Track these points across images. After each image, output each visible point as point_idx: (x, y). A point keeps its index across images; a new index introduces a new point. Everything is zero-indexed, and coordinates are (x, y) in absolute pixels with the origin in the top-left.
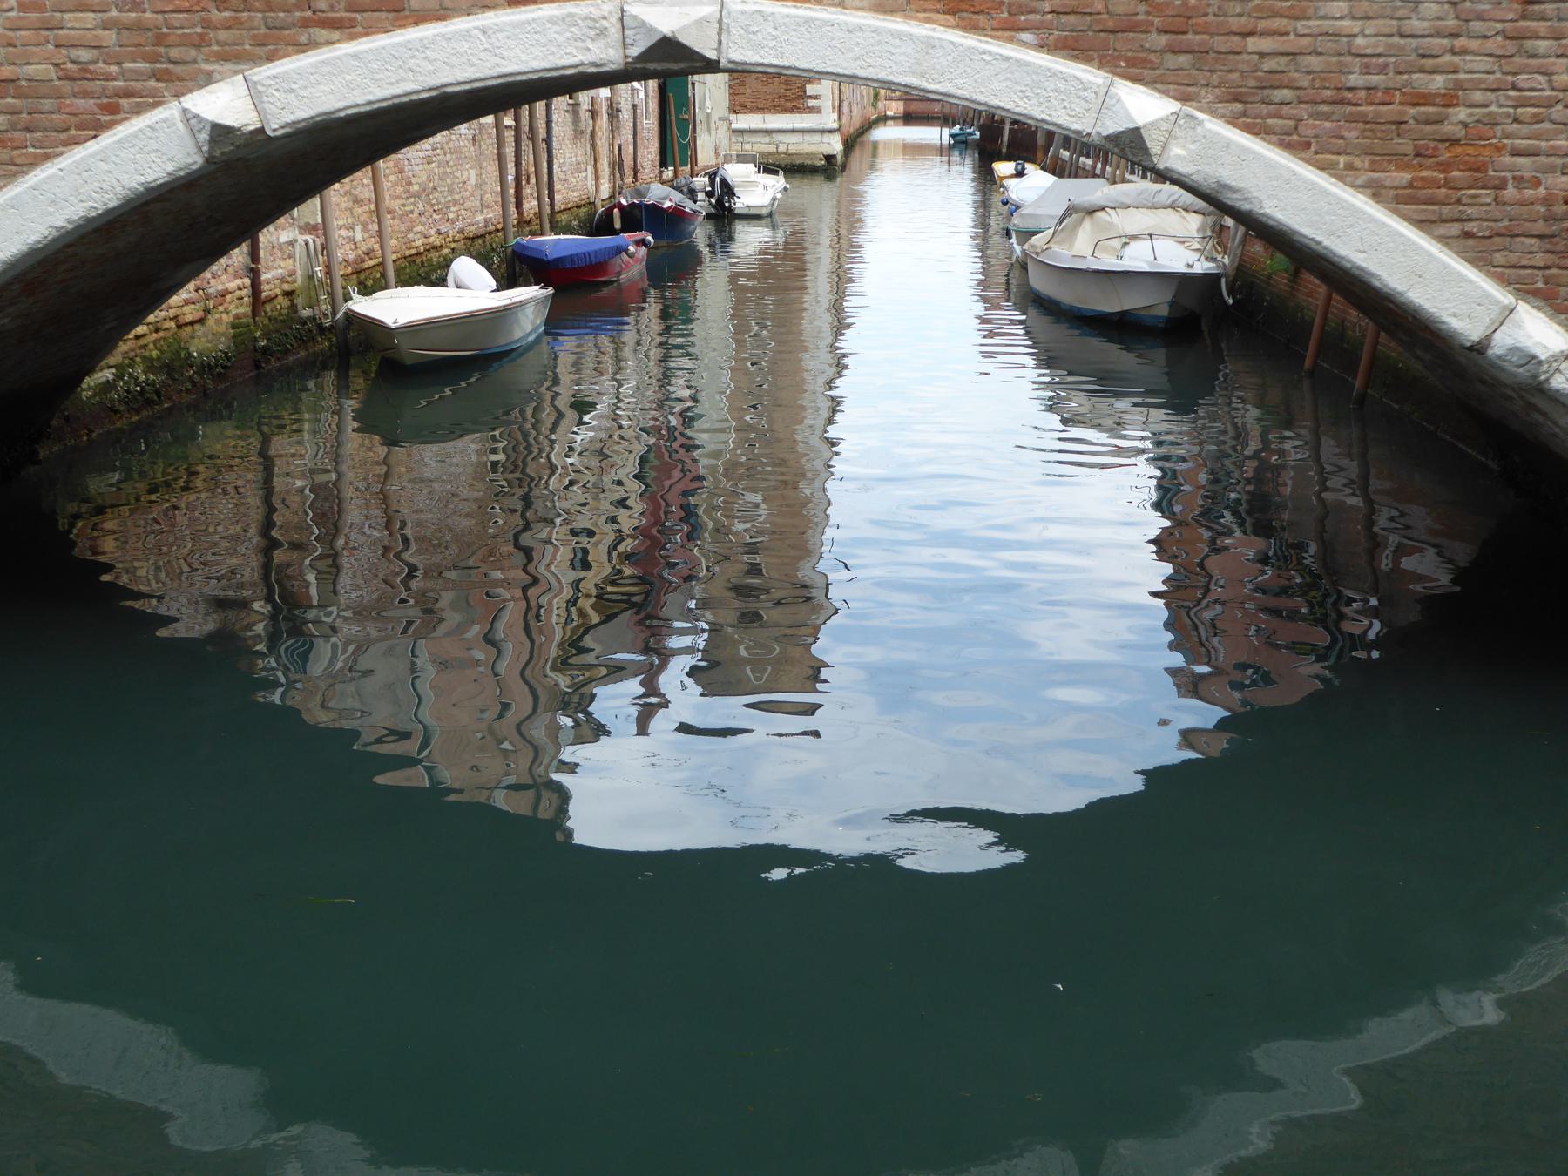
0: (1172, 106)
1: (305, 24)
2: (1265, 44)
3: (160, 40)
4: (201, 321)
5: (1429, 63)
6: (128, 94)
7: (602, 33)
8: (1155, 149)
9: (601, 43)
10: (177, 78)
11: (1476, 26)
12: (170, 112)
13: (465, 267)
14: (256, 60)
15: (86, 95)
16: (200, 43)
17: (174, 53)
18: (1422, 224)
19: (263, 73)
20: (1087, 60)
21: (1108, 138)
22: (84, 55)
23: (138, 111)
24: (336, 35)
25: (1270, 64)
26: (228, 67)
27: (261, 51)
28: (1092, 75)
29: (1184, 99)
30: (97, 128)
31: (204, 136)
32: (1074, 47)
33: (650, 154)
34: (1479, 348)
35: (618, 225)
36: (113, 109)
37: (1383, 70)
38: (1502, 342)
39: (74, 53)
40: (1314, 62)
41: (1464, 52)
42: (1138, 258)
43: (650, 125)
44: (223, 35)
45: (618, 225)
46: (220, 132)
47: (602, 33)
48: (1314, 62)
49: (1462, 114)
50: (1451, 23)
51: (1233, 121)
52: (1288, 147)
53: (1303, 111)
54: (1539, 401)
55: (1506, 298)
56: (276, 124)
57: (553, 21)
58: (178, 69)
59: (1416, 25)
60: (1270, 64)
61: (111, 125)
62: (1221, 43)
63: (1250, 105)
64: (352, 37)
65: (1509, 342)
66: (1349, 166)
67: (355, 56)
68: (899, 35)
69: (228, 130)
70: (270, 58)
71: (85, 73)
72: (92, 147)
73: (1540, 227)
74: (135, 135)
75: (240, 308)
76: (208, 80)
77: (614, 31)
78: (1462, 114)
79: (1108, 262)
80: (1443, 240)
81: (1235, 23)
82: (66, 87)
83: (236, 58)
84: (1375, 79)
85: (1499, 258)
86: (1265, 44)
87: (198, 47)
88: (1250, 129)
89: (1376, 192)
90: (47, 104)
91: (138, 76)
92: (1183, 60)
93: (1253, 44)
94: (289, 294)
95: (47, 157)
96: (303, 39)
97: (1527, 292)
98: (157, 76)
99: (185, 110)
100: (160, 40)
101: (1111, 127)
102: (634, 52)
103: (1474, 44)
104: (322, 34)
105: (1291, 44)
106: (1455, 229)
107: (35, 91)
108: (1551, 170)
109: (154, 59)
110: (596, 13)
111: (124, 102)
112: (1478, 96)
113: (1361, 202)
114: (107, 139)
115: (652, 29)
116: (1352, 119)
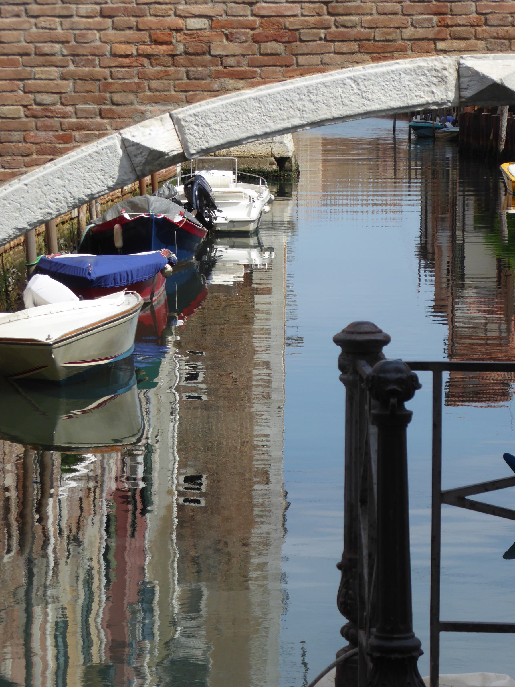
1: (218, 76)
6: (79, 128)
7: (443, 80)
9: (442, 87)
10: (116, 114)
12: (112, 142)
13: (42, 284)
14: (178, 103)
15: (46, 128)
17: (117, 97)
19: (184, 112)
22: (47, 98)
23: (86, 140)
24: (241, 84)
26: (157, 107)
27: (183, 95)
30: (54, 153)
35: (119, 243)
36: (67, 139)
39: (40, 97)
44: (155, 84)
45: (119, 243)
57: (406, 72)
58: (119, 109)
61: (65, 151)
64: (253, 85)
67: (258, 99)
70: (189, 102)
71: (48, 111)
72: (50, 167)
74: (85, 159)
76: (142, 116)
77: (452, 80)
82: (32, 123)
83: (164, 100)
87: (136, 93)
90: (17, 136)
91: (88, 115)
95: (13, 175)
96: (216, 87)
98: (101, 114)
99: (124, 141)
100: (106, 88)
102: (467, 94)
104: (231, 83)
109: (101, 101)
110: (438, 65)
111: (77, 134)
114: (62, 162)
115: (483, 78)
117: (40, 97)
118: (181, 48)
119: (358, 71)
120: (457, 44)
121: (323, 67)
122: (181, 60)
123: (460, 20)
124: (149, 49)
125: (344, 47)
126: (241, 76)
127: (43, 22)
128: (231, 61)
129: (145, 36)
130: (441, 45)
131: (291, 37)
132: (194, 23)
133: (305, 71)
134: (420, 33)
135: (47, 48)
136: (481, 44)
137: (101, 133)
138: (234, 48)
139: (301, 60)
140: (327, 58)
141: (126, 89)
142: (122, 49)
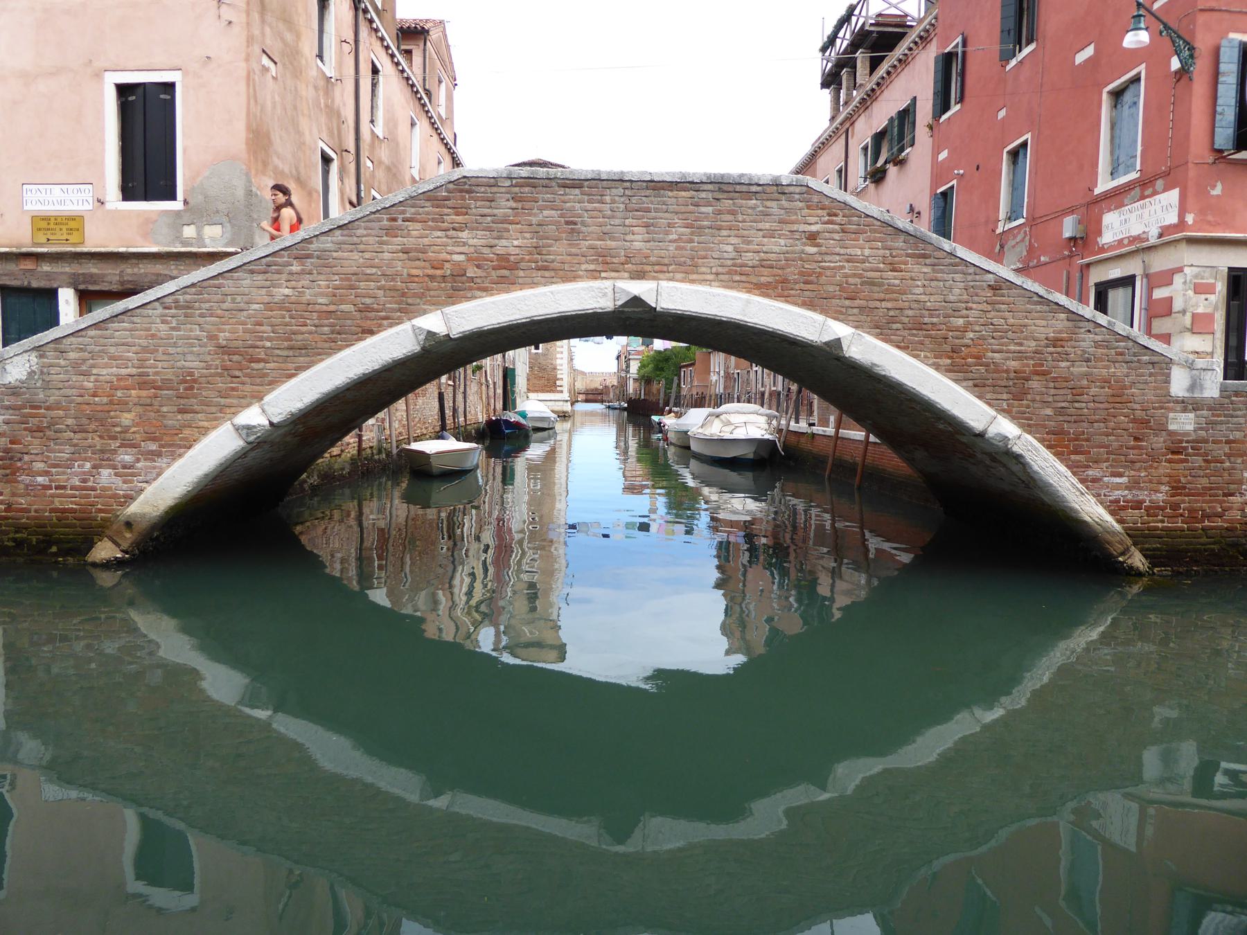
0: (853, 330)
1: (471, 289)
2: (889, 305)
3: (404, 295)
4: (339, 455)
5: (956, 314)
7: (605, 295)
8: (845, 348)
10: (407, 311)
11: (975, 298)
12: (406, 326)
16: (422, 296)
17: (410, 301)
18: (956, 381)
20: (815, 310)
21: (826, 343)
22: (368, 301)
23: (391, 326)
25: (892, 313)
28: (819, 317)
29: (856, 327)
31: (422, 337)
32: (810, 305)
33: (500, 405)
34: (981, 435)
37: (938, 316)
38: (992, 432)
39: (364, 300)
40: (910, 313)
41: (971, 309)
42: (740, 434)
43: (500, 391)
46: (430, 334)
47: (605, 295)
48: (910, 313)
49: (971, 335)
50: (965, 297)
51: (877, 336)
52: (899, 347)
53: (906, 333)
54: (1004, 459)
55: (994, 413)
56: (455, 334)
57: (583, 289)
59: (951, 298)
60: (892, 313)
61: (379, 332)
62: (873, 304)
63: (883, 330)
64: (492, 295)
65: (996, 431)
66: (926, 357)
68: (735, 298)
69: (435, 334)
73: (1004, 383)
75: (352, 451)
76: (425, 312)
78: (971, 335)
79: (727, 436)
80: (966, 388)
81: (876, 296)
82: (358, 315)
83: (438, 304)
84: (935, 320)
85: (989, 396)
86: (889, 305)
88: (883, 340)
89: (937, 367)
90: (349, 322)
91: (393, 310)
92: (856, 311)
93: (884, 304)
94: (371, 447)
95: (348, 346)
97: (1001, 411)
98: (400, 310)
100: (404, 295)
101: (826, 338)
102: (619, 303)
103: (974, 306)
104: (479, 293)
105: (900, 304)
106: (971, 383)
107: (346, 315)
108: (1008, 359)
111: (385, 322)
112: (977, 328)
113: (932, 371)
115: (629, 293)
116: (926, 336)
117: (364, 300)
118: (449, 272)
119: (554, 287)
120: (613, 274)
121: (534, 284)
122: (449, 279)
123: (614, 260)
124: (431, 272)
125: (547, 274)
126: (485, 290)
127: (367, 255)
128: (478, 280)
129: (427, 264)
130: (603, 275)
131: (514, 267)
132: (456, 258)
133: (523, 286)
134: (592, 267)
135: (368, 271)
136: (626, 275)
137: (399, 321)
138: (479, 273)
139: (520, 280)
140: (535, 280)
141: (415, 295)
142: (414, 272)
